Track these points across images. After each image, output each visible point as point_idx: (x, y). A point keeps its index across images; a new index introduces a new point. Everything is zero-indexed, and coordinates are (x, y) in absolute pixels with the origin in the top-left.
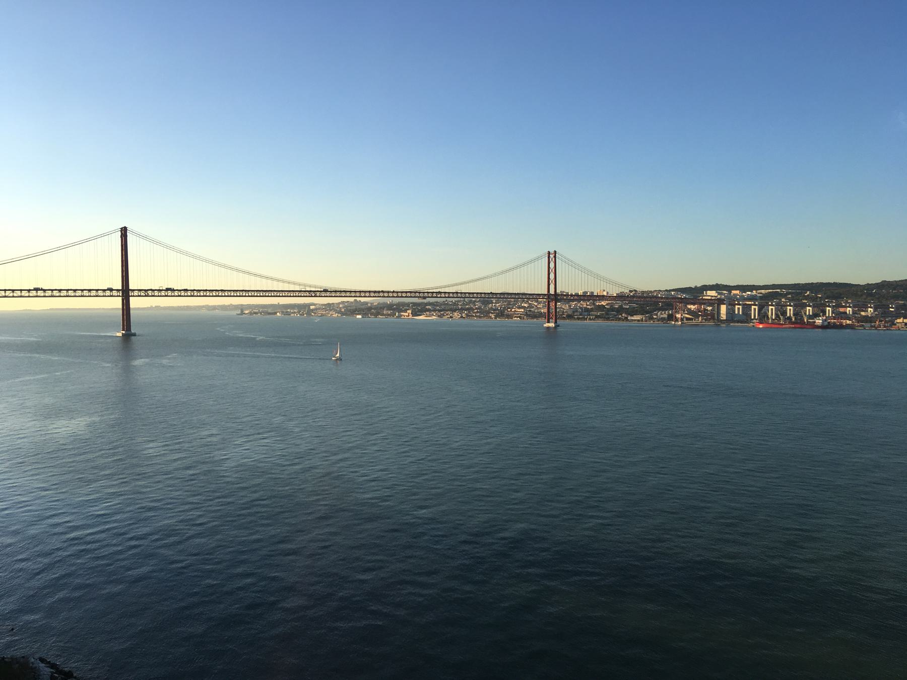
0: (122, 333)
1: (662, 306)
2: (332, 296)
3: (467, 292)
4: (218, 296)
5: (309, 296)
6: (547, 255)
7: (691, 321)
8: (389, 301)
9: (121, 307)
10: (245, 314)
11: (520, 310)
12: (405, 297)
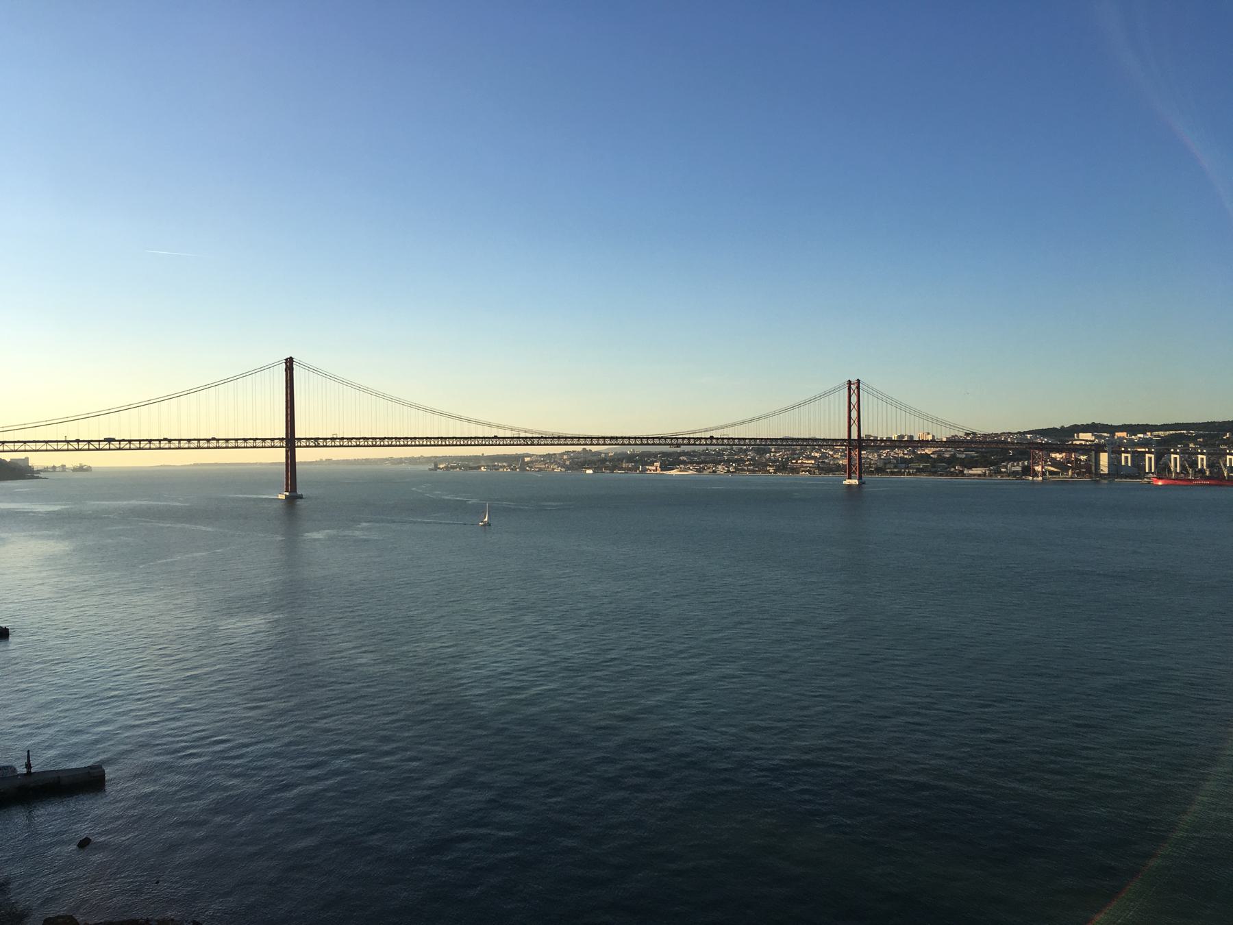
0: (286, 495)
2: (554, 445)
3: (736, 437)
4: (407, 445)
7: (1057, 476)
8: (629, 450)
9: (284, 460)
10: (439, 468)
11: (810, 462)
12: (652, 444)
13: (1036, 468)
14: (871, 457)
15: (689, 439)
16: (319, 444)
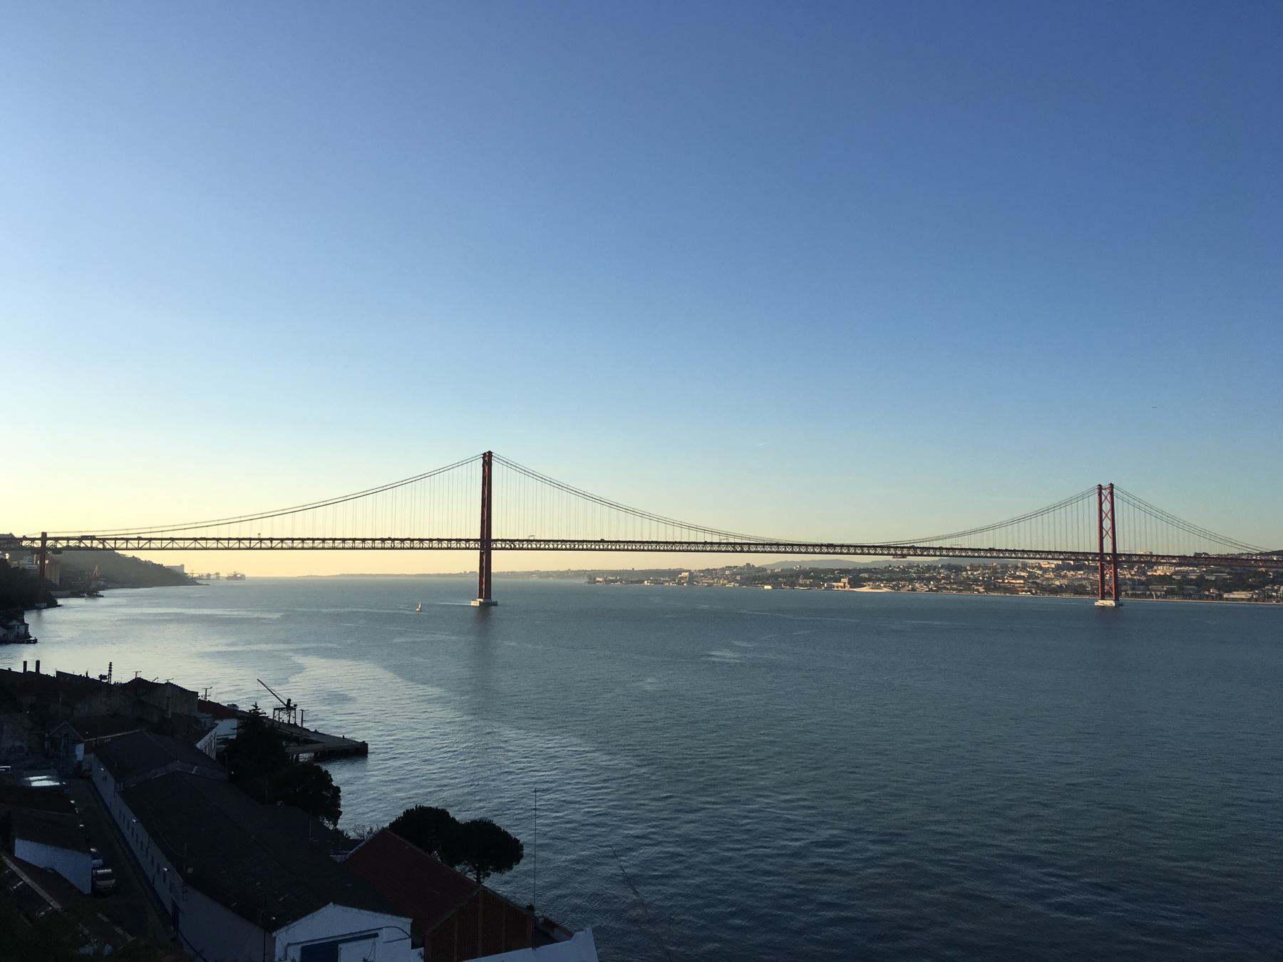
0: (480, 602)
1: (1274, 577)
5: (733, 552)
6: (1097, 491)
10: (598, 582)
11: (1018, 581)
14: (1125, 574)
16: (515, 546)
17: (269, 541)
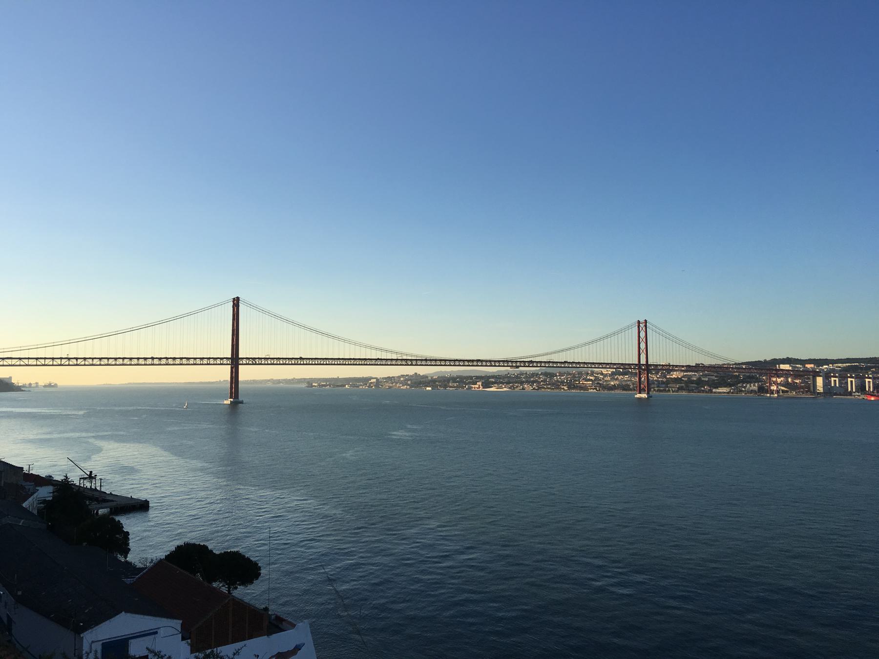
0: (231, 401)
1: (743, 379)
5: (406, 365)
10: (314, 386)
11: (588, 383)
13: (772, 388)
14: (654, 377)
15: (524, 362)
17: (75, 360)
